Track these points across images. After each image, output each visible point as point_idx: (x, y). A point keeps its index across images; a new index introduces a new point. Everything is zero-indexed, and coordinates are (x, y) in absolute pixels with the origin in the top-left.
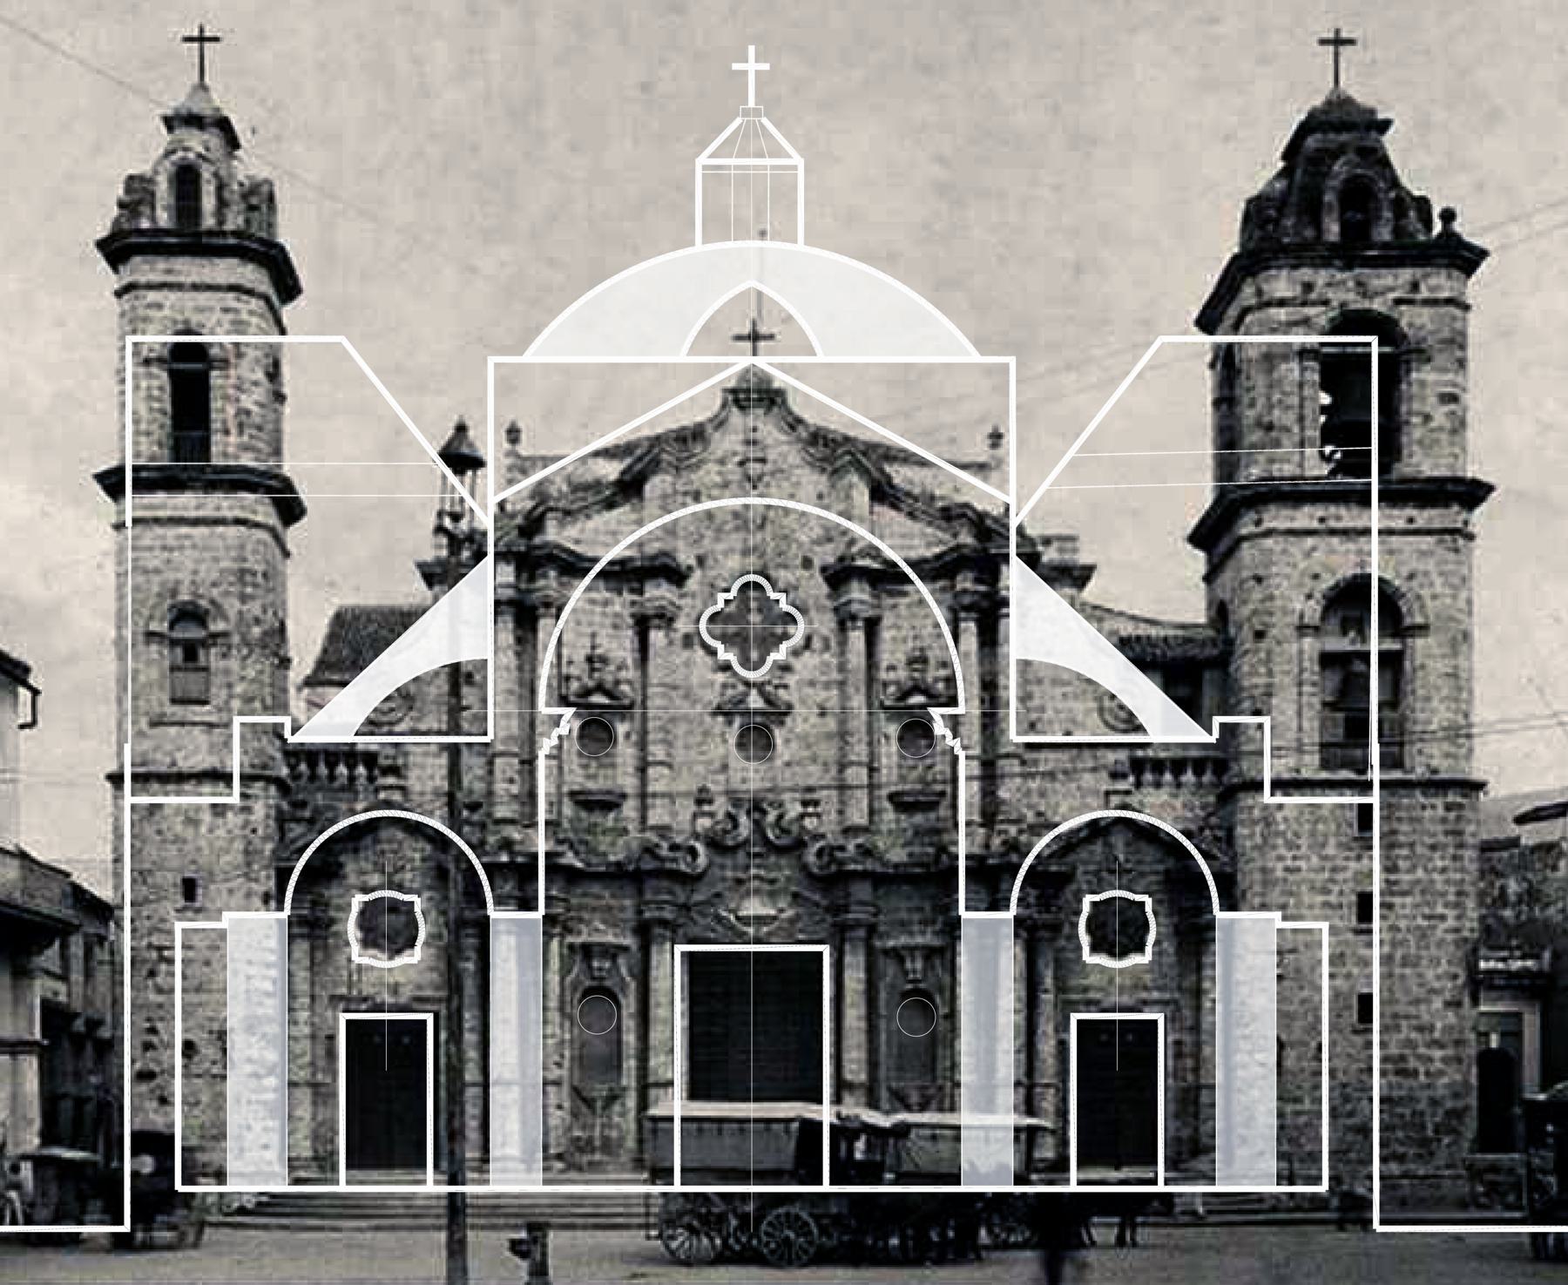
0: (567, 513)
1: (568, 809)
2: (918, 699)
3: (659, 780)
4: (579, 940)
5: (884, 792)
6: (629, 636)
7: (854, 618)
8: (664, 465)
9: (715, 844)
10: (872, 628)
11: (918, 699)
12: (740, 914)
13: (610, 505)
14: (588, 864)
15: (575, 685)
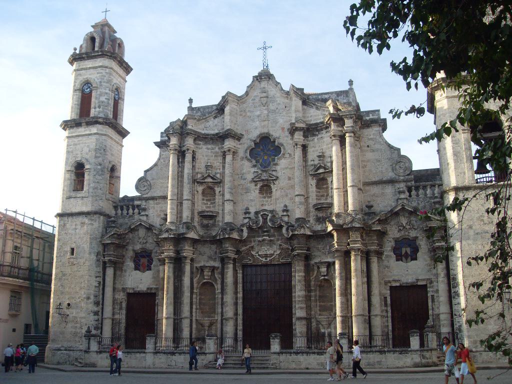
0: (199, 120)
1: (196, 219)
2: (321, 171)
3: (228, 207)
4: (198, 265)
5: (311, 206)
6: (220, 159)
7: (296, 144)
8: (229, 102)
9: (250, 228)
10: (304, 147)
11: (321, 171)
12: (260, 253)
13: (215, 117)
14: (202, 238)
15: (199, 176)
